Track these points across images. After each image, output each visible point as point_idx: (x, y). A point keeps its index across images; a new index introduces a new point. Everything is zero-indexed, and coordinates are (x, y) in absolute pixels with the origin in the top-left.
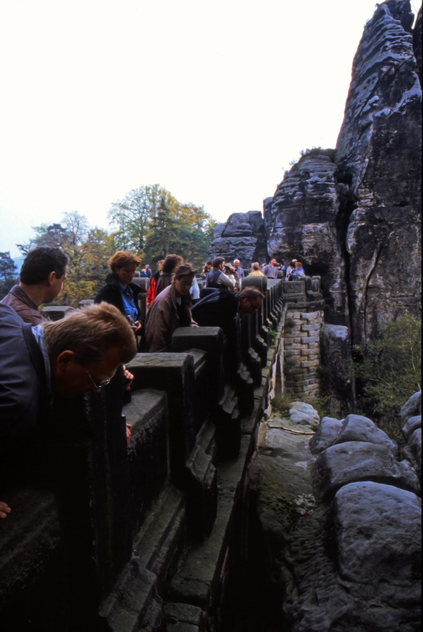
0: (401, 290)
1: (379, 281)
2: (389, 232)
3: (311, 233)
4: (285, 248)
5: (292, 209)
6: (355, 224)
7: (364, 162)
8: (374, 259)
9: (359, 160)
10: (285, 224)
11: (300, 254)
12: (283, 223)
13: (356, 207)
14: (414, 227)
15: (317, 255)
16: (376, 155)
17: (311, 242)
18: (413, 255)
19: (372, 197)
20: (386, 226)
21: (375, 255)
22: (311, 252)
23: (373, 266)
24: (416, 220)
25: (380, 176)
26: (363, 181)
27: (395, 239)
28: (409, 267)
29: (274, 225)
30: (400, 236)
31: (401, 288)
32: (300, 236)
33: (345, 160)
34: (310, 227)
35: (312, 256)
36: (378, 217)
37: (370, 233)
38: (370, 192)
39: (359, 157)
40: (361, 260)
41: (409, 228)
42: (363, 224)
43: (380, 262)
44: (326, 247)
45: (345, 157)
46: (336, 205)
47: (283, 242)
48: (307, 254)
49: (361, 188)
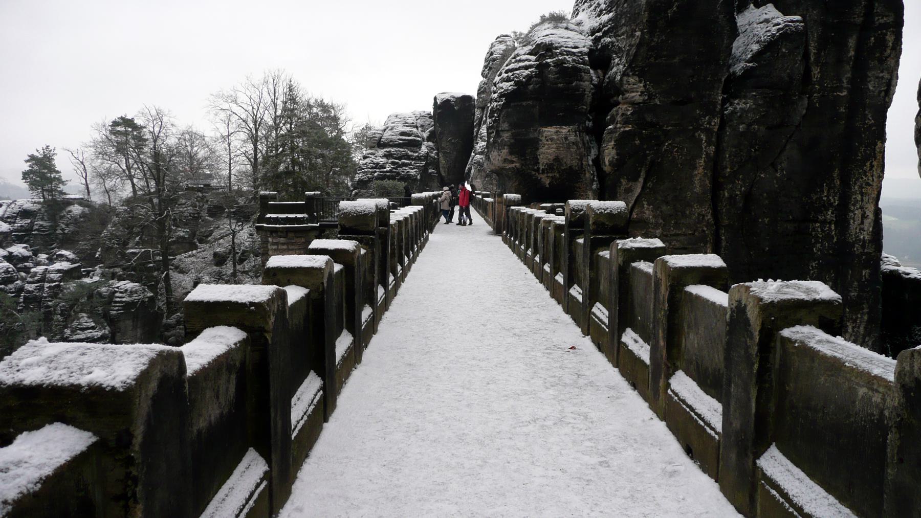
0: (677, 226)
1: (647, 212)
2: (663, 143)
3: (552, 140)
4: (512, 162)
5: (524, 104)
6: (615, 128)
7: (632, 36)
8: (641, 180)
9: (623, 34)
10: (513, 126)
11: (534, 170)
12: (510, 125)
13: (618, 103)
14: (699, 135)
15: (559, 172)
16: (652, 26)
17: (551, 154)
18: (696, 175)
19: (642, 89)
20: (660, 133)
21: (643, 174)
22: (550, 168)
23: (639, 190)
24: (702, 125)
25: (656, 59)
26: (630, 66)
27: (672, 152)
28: (689, 194)
29: (497, 127)
30: (679, 148)
31: (676, 223)
32: (535, 144)
33: (598, 34)
34: (550, 131)
35: (550, 175)
36: (649, 119)
37: (637, 142)
38: (640, 82)
39: (624, 29)
40: (624, 182)
41: (693, 136)
42: (627, 129)
43: (649, 184)
44: (570, 160)
45: (599, 30)
46: (588, 98)
47: (511, 153)
48: (543, 173)
49: (628, 76)
